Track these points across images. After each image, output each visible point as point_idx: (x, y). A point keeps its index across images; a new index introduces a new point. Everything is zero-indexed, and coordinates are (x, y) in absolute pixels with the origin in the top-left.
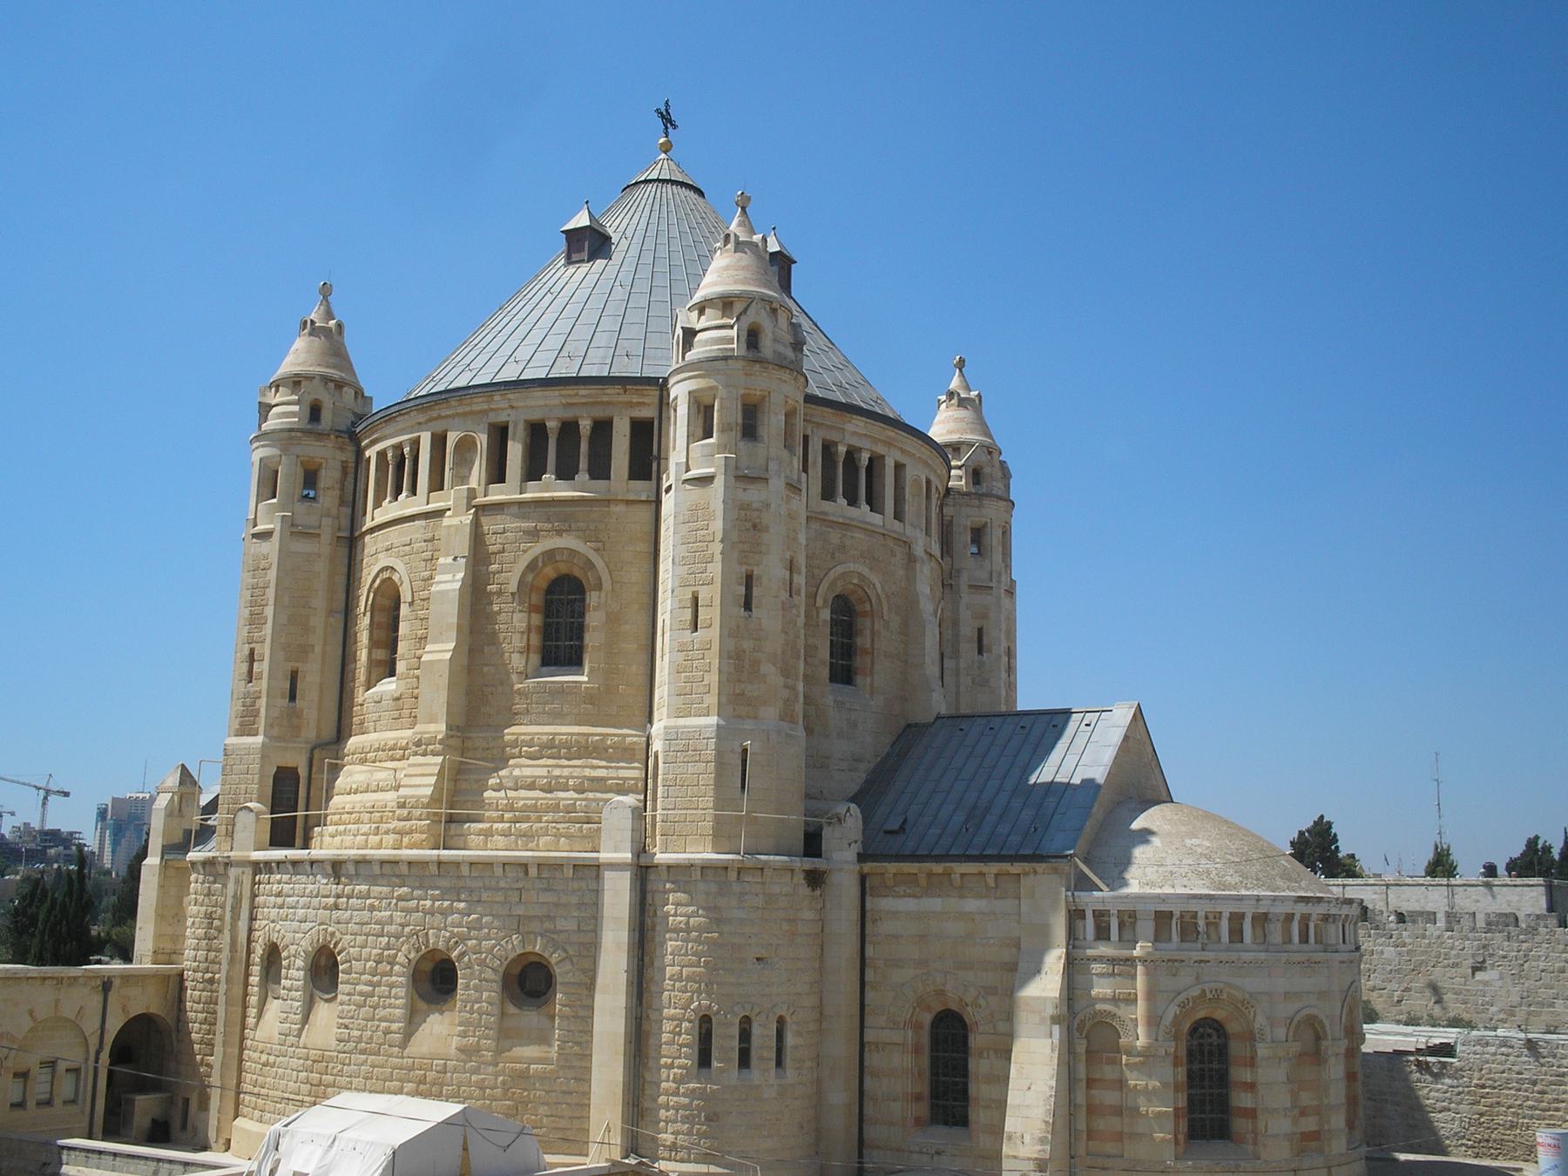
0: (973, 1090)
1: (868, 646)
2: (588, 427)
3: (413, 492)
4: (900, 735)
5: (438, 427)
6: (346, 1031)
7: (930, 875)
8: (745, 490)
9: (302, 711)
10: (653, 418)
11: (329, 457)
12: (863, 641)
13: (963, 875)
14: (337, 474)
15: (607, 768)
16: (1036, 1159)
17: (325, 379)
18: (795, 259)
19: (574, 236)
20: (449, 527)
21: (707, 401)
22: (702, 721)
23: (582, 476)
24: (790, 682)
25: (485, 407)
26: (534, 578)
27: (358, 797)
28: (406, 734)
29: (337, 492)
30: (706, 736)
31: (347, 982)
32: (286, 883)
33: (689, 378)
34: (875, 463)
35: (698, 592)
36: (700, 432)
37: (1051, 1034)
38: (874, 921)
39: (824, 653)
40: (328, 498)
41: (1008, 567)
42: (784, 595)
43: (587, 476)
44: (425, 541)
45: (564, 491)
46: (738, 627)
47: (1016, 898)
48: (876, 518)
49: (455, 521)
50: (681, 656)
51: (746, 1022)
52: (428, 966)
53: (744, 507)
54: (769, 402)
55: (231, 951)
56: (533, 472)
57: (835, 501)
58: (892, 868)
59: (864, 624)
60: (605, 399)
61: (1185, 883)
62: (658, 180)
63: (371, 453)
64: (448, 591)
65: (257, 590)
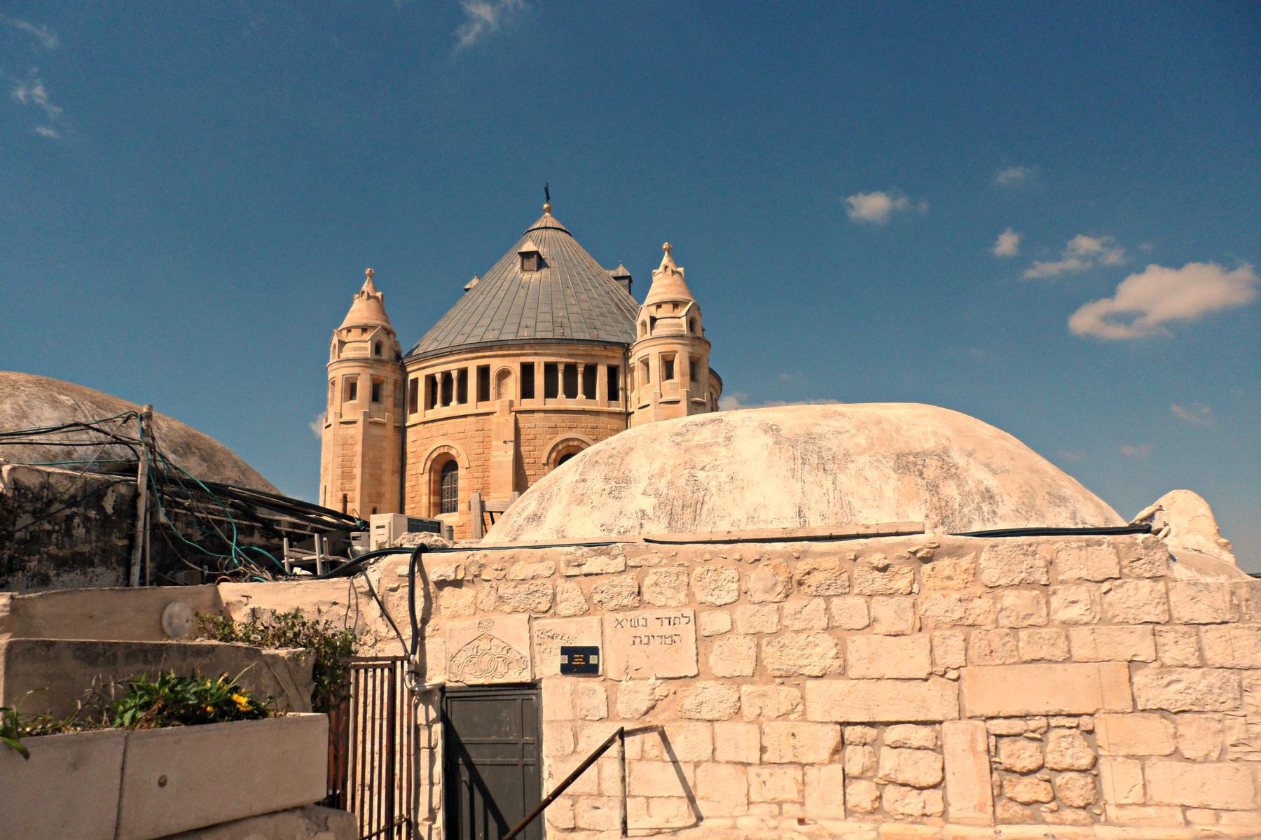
3: (463, 399)
5: (483, 362)
10: (618, 366)
19: (526, 256)
21: (669, 359)
25: (518, 352)
33: (672, 344)
36: (665, 377)
43: (584, 397)
45: (571, 404)
49: (502, 420)
60: (594, 353)
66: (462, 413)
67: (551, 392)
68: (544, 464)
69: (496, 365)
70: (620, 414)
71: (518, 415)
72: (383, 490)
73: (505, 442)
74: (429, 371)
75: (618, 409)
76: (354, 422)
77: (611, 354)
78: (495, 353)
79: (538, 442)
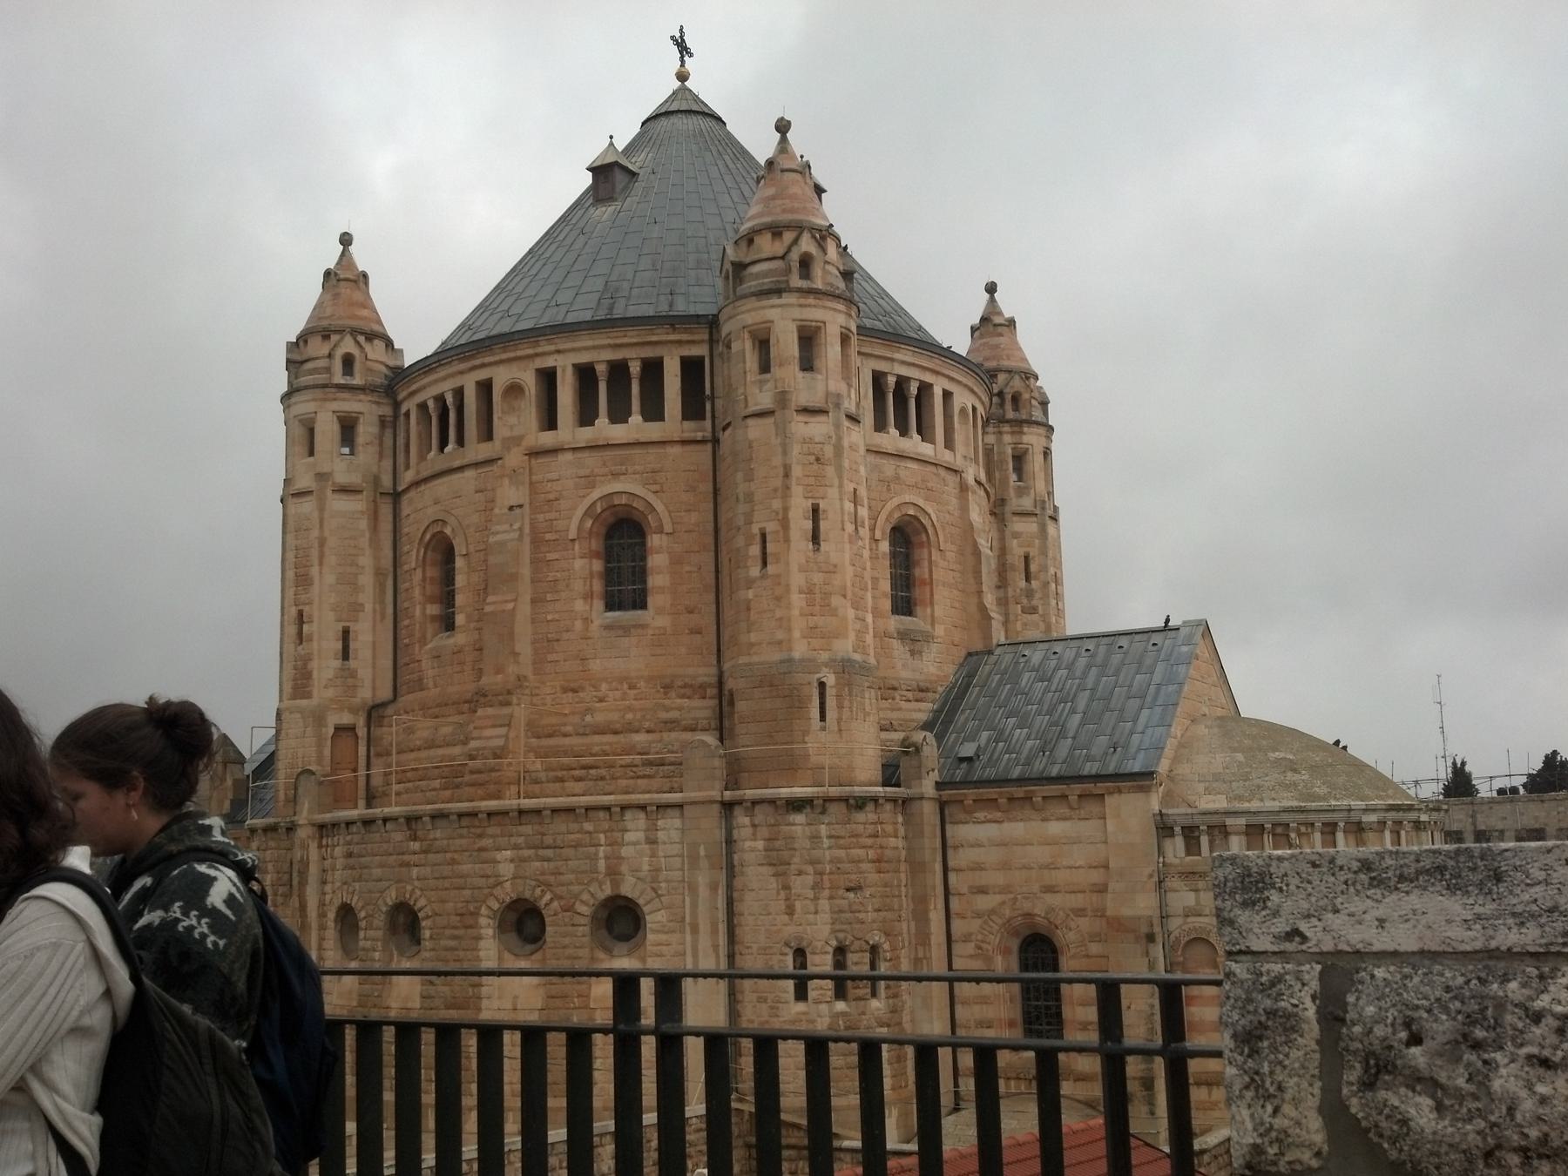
0: (1067, 1013)
1: (927, 576)
2: (638, 369)
3: (461, 441)
4: (962, 665)
5: (482, 375)
6: (431, 987)
7: (1011, 799)
10: (703, 357)
11: (367, 411)
12: (921, 572)
13: (1044, 798)
14: (375, 430)
16: (1142, 1078)
17: (355, 332)
18: (826, 188)
23: (636, 418)
24: (860, 613)
25: (530, 351)
26: (592, 525)
27: (423, 754)
29: (376, 448)
32: (357, 844)
34: (925, 388)
35: (765, 528)
37: (1147, 952)
38: (956, 848)
39: (886, 585)
40: (366, 455)
41: (1050, 494)
42: (850, 528)
43: (640, 418)
44: (476, 492)
45: (618, 433)
46: (807, 562)
47: (1100, 818)
48: (926, 450)
52: (512, 917)
53: (808, 441)
57: (888, 433)
58: (971, 793)
59: (921, 554)
60: (654, 338)
61: (1273, 796)
62: (679, 111)
63: (410, 405)
65: (301, 552)
66: (457, 463)
67: (586, 416)
68: (573, 540)
70: (703, 442)
71: (533, 461)
72: (362, 598)
73: (511, 508)
74: (419, 398)
75: (699, 436)
77: (685, 337)
78: (497, 358)
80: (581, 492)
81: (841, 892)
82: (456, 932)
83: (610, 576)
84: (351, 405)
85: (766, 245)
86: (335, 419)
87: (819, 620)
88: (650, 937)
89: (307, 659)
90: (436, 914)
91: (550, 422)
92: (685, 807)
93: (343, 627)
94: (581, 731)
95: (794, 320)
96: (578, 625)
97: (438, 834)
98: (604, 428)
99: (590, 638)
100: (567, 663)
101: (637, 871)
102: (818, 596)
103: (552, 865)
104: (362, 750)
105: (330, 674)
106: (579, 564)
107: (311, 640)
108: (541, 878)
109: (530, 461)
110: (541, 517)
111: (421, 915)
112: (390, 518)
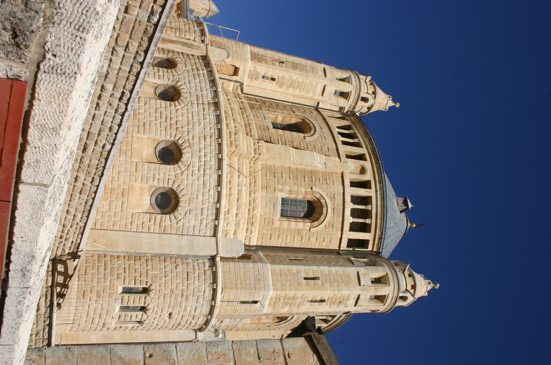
3: (344, 143)
6: (144, 103)
8: (354, 298)
9: (258, 80)
10: (367, 248)
14: (341, 105)
15: (243, 229)
20: (336, 161)
21: (383, 280)
22: (271, 283)
23: (352, 220)
28: (255, 133)
29: (334, 104)
30: (265, 285)
31: (166, 107)
35: (319, 280)
49: (338, 164)
50: (295, 271)
51: (143, 309)
54: (381, 305)
55: (168, 40)
56: (356, 200)
62: (407, 225)
64: (315, 160)
65: (305, 67)
68: (312, 189)
69: (367, 165)
70: (340, 246)
71: (340, 175)
72: (284, 88)
75: (342, 245)
76: (326, 76)
77: (376, 242)
79: (325, 186)
80: (329, 195)
81: (171, 311)
82: (169, 119)
83: (294, 202)
84: (352, 98)
85: (410, 282)
86: (349, 91)
87: (281, 302)
88: (159, 216)
89: (266, 62)
90: (177, 111)
91: (354, 184)
92: (215, 238)
93: (275, 79)
94: (239, 184)
95: (388, 294)
96: (280, 187)
97: (212, 117)
98: (350, 206)
99: (275, 191)
100: (265, 180)
101: (189, 213)
102: (291, 301)
103: (197, 172)
104: (227, 77)
105: (259, 70)
106: (303, 189)
107: (273, 64)
108: (191, 166)
109: (340, 173)
110: (320, 175)
111: (176, 102)
112: (310, 105)
